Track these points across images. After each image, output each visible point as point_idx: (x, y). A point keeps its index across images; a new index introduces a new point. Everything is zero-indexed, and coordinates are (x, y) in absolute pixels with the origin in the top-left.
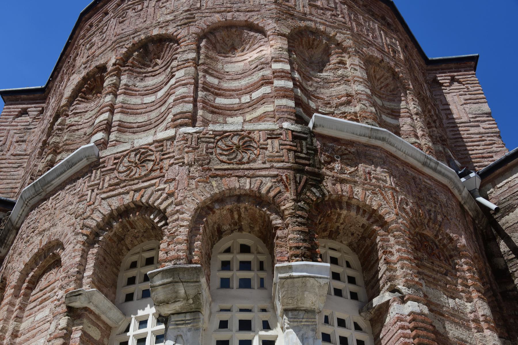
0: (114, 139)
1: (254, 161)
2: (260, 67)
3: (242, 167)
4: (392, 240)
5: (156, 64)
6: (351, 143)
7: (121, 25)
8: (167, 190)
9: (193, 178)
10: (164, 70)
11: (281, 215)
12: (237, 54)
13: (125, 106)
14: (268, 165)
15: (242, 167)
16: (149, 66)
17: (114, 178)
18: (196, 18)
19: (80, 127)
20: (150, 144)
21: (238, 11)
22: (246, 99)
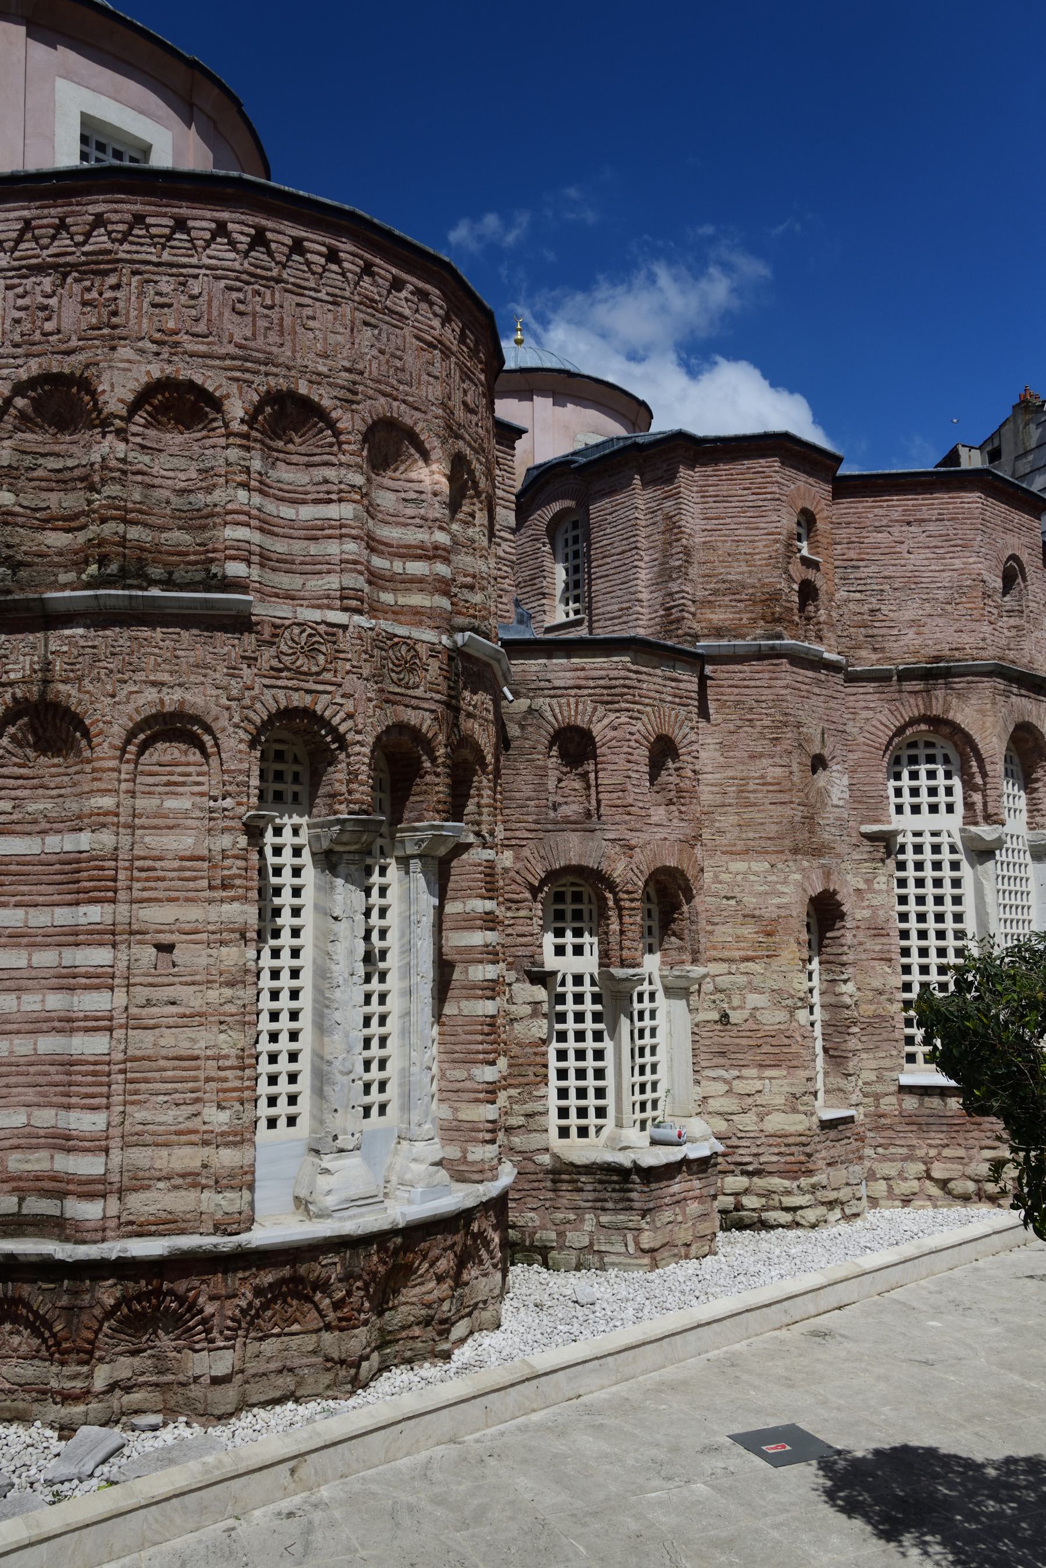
0: (256, 579)
1: (418, 687)
2: (418, 521)
3: (410, 692)
4: (485, 782)
5: (291, 441)
6: (477, 659)
7: (236, 318)
8: (346, 709)
9: (370, 700)
10: (308, 465)
11: (433, 760)
12: (389, 473)
13: (262, 516)
14: (428, 695)
15: (410, 692)
16: (280, 439)
17: (274, 657)
18: (360, 397)
19: (157, 481)
20: (318, 623)
21: (404, 402)
22: (398, 566)
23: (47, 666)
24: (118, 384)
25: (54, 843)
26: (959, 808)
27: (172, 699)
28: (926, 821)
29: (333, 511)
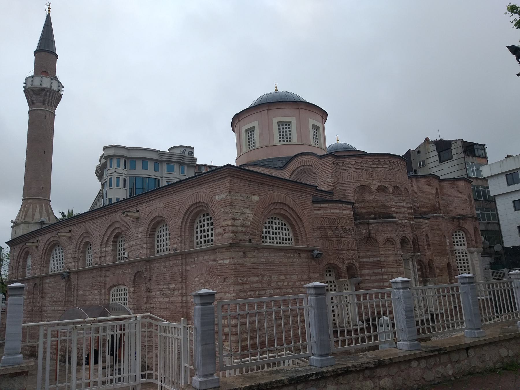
23: (369, 231)
24: (374, 187)
25: (371, 259)
26: (466, 244)
27: (389, 235)
28: (459, 247)
29: (402, 204)
